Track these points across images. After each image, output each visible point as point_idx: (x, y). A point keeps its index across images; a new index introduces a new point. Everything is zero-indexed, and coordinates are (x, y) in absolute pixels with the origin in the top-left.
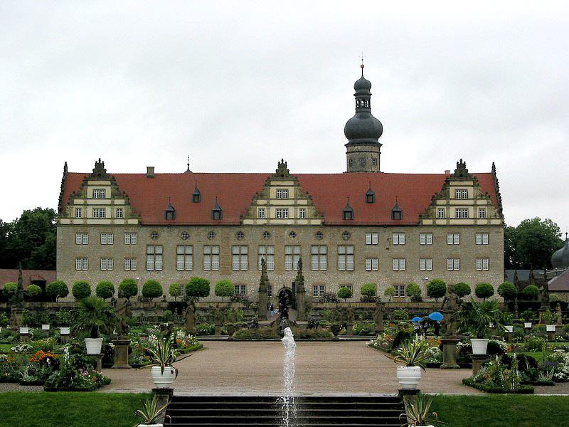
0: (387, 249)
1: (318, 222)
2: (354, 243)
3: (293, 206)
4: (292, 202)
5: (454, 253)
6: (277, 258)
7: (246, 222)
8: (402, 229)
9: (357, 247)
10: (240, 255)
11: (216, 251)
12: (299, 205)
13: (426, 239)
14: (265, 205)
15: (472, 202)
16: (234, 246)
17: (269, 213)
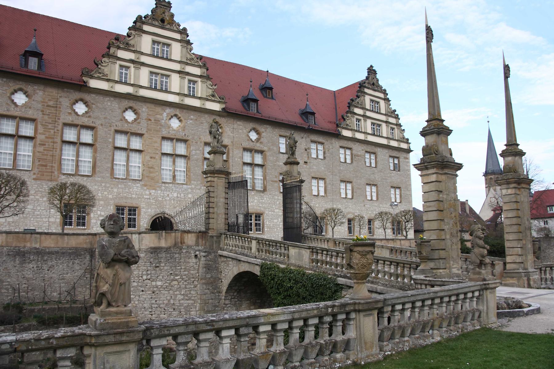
0: (306, 162)
1: (216, 107)
2: (265, 148)
3: (179, 72)
4: (177, 67)
5: (372, 177)
6: (148, 158)
7: (94, 84)
8: (321, 139)
9: (268, 154)
10: (78, 144)
11: (27, 129)
12: (188, 74)
13: (344, 155)
14: (132, 61)
15: (383, 118)
16: (65, 125)
17: (137, 77)
